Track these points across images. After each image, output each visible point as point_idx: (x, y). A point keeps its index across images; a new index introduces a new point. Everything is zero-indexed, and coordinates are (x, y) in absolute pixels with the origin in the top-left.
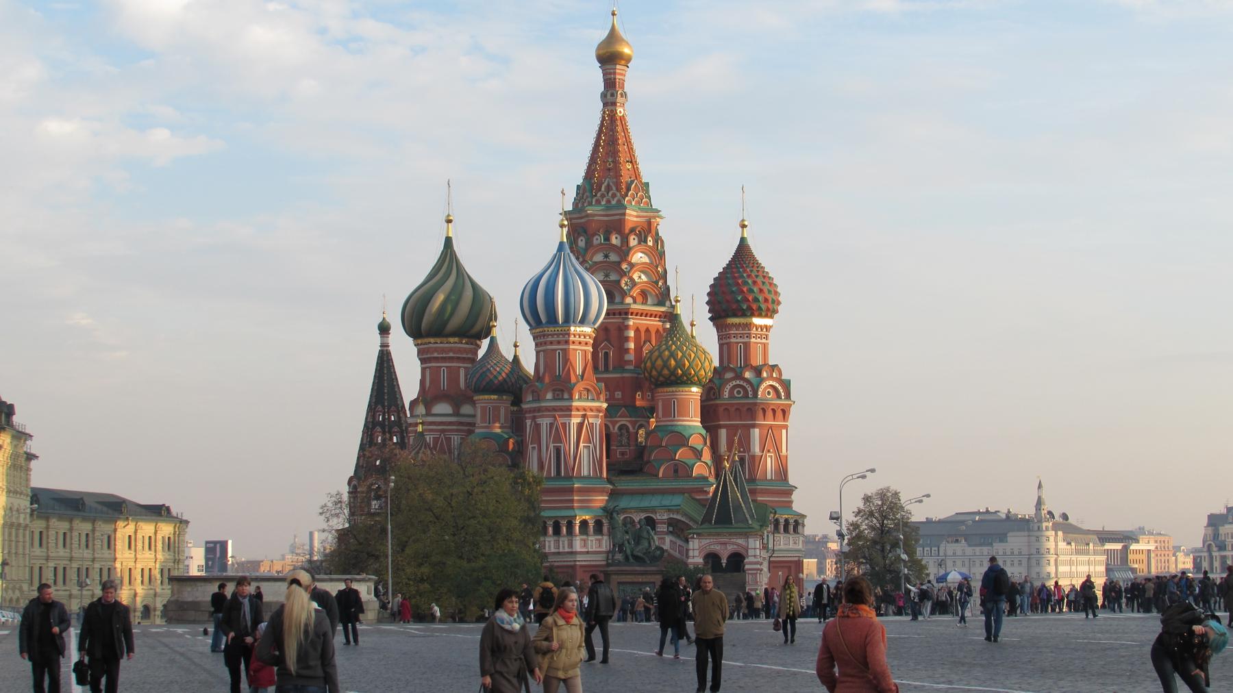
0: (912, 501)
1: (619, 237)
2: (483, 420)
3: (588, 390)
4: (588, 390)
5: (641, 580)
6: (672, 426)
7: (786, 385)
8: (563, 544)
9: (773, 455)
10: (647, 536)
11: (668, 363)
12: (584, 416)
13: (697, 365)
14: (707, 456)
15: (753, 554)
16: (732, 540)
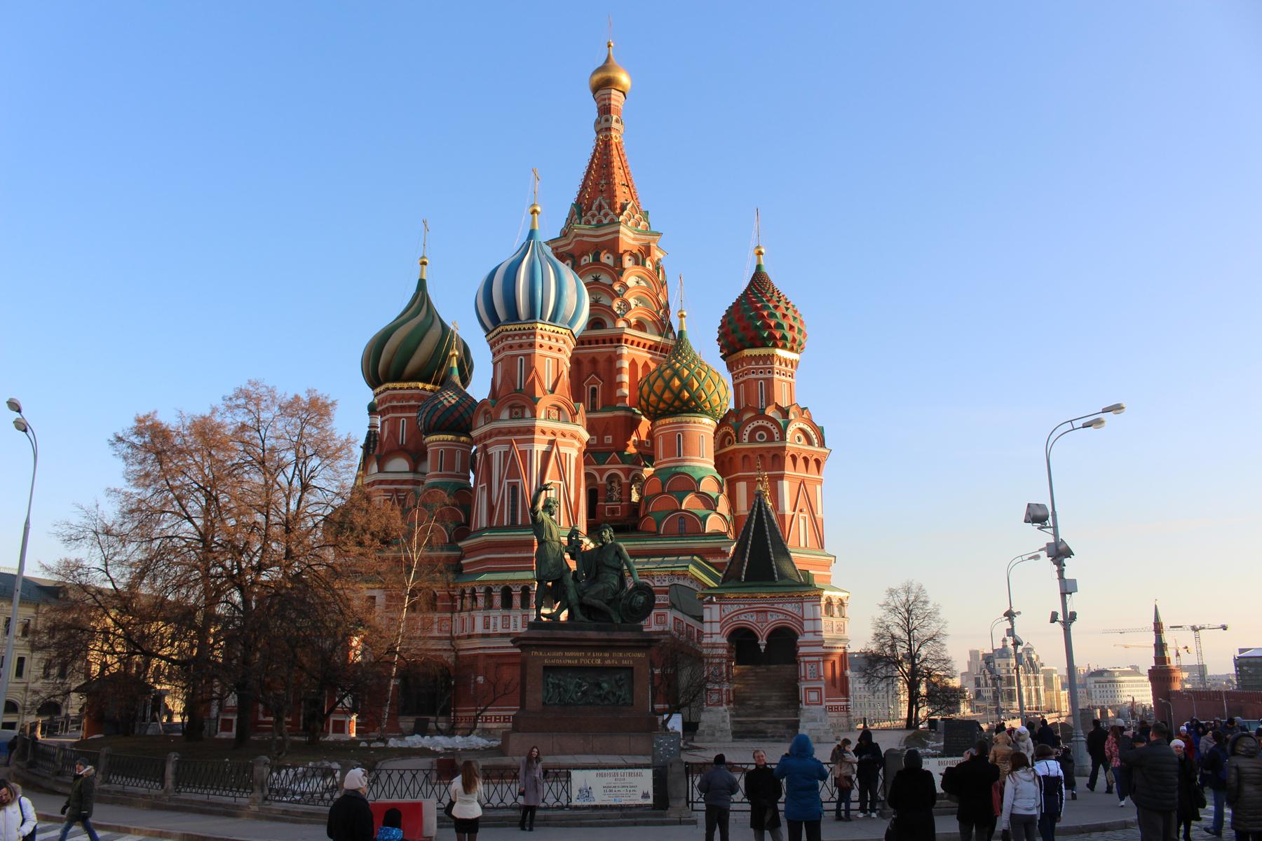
0: (1025, 558)
1: (611, 257)
2: (434, 469)
3: (559, 409)
4: (559, 409)
5: (599, 662)
6: (677, 467)
7: (820, 432)
8: (515, 621)
9: (807, 516)
10: (617, 565)
11: (671, 384)
12: (552, 443)
13: (709, 387)
14: (723, 506)
15: (812, 630)
16: (776, 606)
